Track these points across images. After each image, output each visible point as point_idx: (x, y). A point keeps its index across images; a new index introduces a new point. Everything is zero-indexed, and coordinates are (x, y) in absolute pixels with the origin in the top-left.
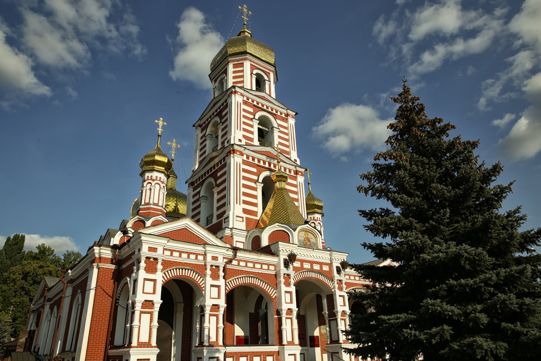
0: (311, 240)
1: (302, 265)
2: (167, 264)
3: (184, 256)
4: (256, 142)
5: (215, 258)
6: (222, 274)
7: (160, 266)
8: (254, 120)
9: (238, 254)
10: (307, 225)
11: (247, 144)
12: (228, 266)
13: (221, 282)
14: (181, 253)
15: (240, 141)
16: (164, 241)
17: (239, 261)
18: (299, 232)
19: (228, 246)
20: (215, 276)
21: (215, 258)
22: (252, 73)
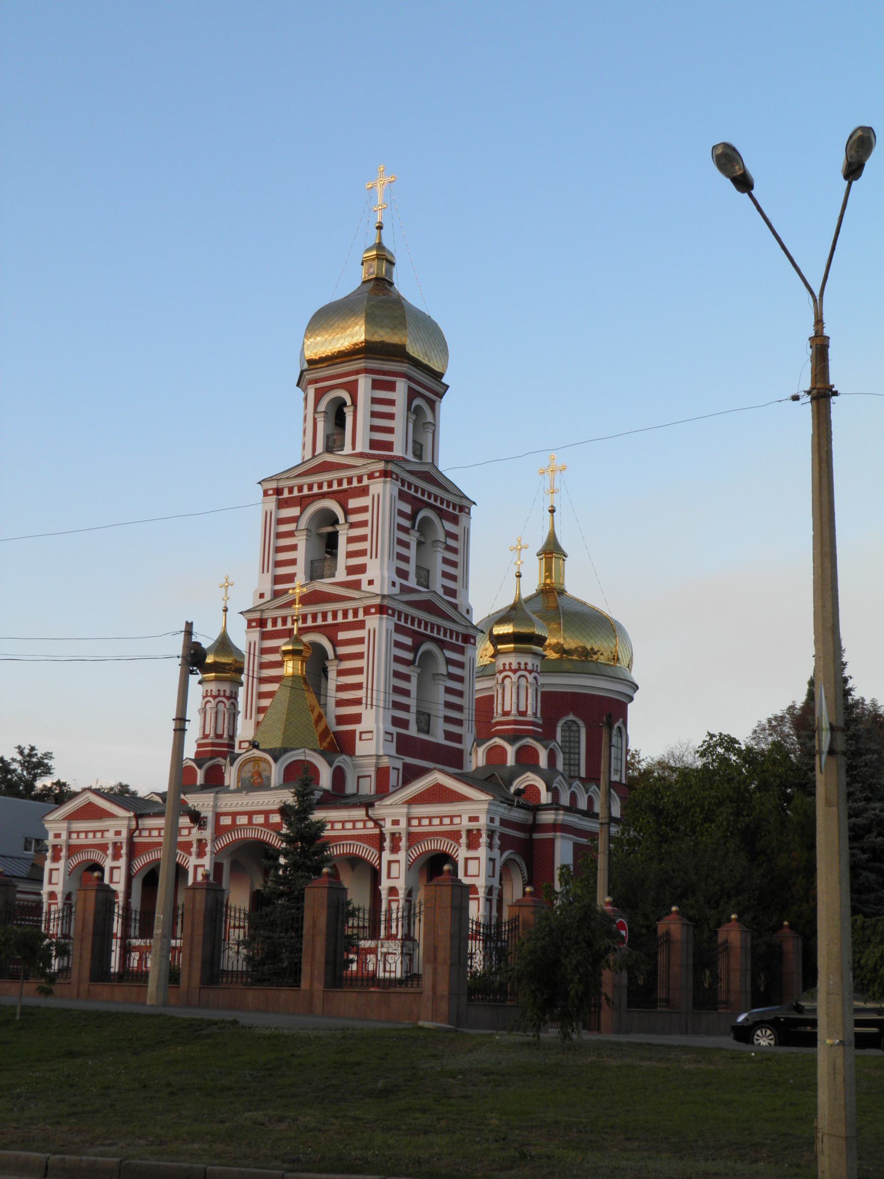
0: (264, 774)
1: (234, 820)
2: (73, 850)
3: (91, 835)
4: (301, 579)
5: (118, 833)
6: (124, 851)
7: (63, 854)
8: (296, 533)
9: (140, 822)
10: (255, 751)
11: (276, 594)
12: (136, 840)
13: (122, 862)
14: (86, 832)
15: (262, 596)
16: (65, 825)
17: (150, 830)
18: (242, 766)
19: (132, 814)
20: (116, 856)
21: (118, 833)
22: (315, 412)
